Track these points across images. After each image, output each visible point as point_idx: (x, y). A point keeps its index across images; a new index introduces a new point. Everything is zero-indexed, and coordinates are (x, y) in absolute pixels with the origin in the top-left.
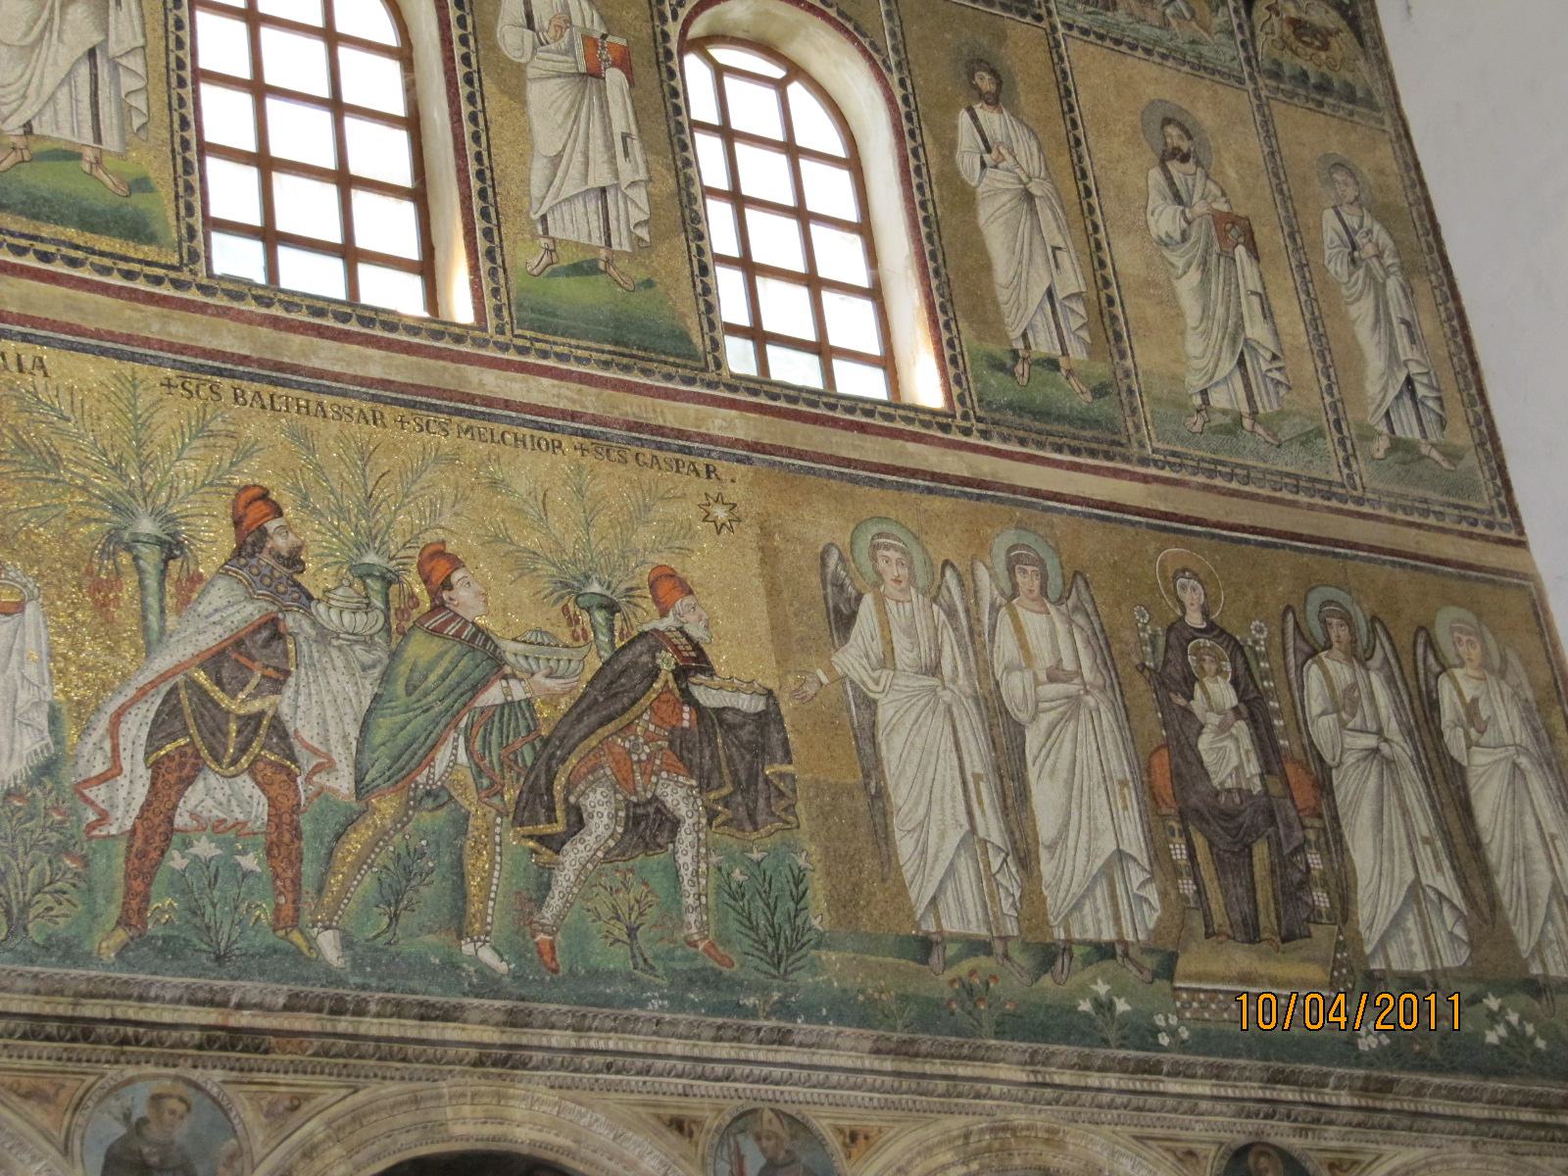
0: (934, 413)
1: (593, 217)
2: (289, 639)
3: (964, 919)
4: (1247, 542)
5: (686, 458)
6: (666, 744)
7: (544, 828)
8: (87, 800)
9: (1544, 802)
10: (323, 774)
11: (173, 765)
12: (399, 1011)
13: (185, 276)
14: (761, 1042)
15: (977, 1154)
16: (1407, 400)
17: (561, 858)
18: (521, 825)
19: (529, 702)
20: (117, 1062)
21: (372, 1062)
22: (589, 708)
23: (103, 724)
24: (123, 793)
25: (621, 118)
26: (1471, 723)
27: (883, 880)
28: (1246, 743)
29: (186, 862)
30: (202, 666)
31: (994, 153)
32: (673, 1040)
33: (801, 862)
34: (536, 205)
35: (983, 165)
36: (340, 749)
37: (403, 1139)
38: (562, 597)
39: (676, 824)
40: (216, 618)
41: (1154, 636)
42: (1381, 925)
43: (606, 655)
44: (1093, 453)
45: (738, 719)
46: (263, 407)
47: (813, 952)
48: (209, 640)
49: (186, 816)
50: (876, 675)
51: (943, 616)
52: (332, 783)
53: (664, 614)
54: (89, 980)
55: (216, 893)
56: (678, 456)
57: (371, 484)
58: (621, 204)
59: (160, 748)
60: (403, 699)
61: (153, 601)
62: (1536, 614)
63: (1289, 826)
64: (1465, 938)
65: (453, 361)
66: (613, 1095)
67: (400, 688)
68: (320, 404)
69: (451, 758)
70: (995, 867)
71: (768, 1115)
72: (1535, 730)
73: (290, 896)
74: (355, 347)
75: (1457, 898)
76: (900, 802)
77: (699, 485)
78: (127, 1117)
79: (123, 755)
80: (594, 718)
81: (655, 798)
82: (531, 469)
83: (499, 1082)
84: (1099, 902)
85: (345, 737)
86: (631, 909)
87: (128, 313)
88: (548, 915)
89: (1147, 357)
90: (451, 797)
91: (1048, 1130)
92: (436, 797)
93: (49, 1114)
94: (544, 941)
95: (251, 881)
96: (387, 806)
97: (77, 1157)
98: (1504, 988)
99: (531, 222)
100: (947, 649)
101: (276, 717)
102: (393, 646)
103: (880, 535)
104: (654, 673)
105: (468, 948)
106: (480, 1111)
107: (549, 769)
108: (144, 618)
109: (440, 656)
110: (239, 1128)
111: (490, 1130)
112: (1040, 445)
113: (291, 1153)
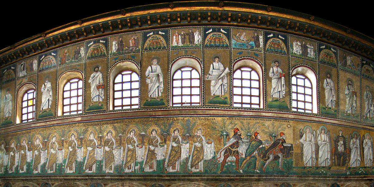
0: (316, 114)
3: (310, 165)
12: (247, 176)
23: (219, 153)
44: (333, 118)
48: (231, 144)
61: (225, 141)
67: (251, 147)
70: (314, 160)
77: (286, 123)
85: (244, 152)
89: (341, 107)
104: (279, 143)
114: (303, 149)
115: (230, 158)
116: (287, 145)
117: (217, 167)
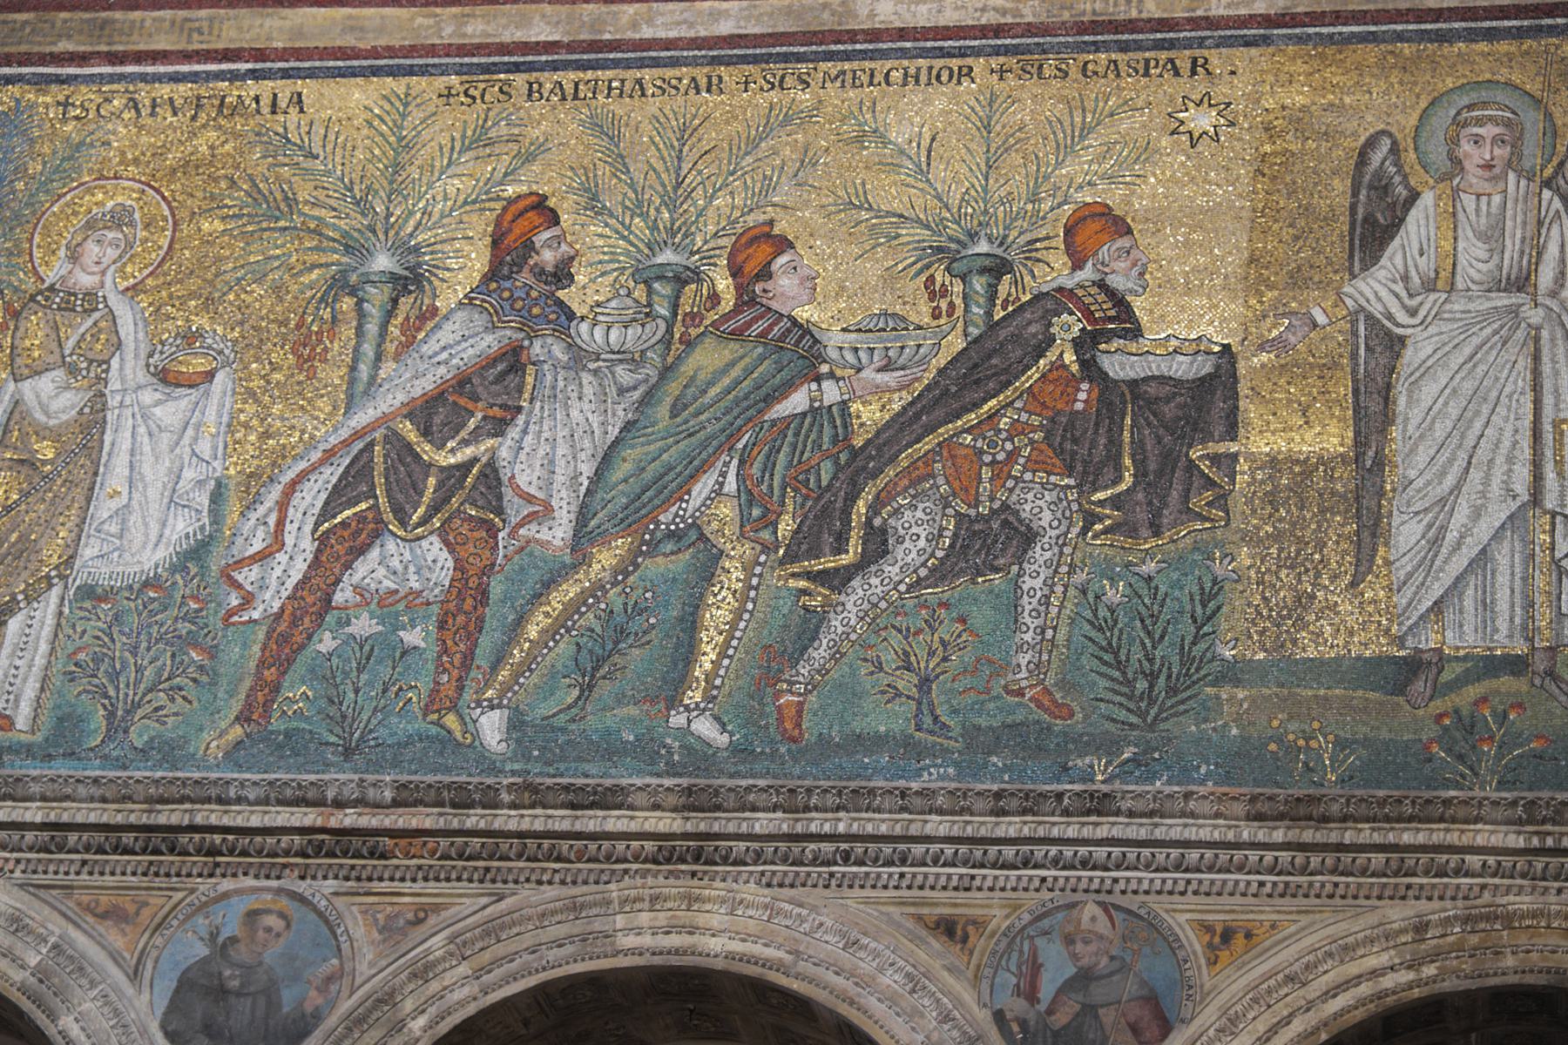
2: (530, 369)
5: (1163, 56)
6: (1038, 436)
7: (828, 562)
10: (534, 527)
11: (346, 534)
14: (1066, 813)
15: (1434, 956)
17: (842, 598)
20: (211, 875)
21: (521, 864)
22: (937, 401)
23: (275, 493)
27: (1353, 584)
29: (334, 644)
30: (410, 416)
32: (934, 817)
36: (564, 494)
37: (553, 954)
38: (928, 267)
39: (1029, 537)
40: (444, 355)
43: (974, 332)
48: (426, 385)
49: (349, 594)
50: (1413, 303)
51: (1557, 204)
52: (545, 535)
53: (1077, 266)
54: (157, 782)
55: (364, 677)
56: (1147, 55)
57: (686, 167)
59: (334, 517)
61: (368, 349)
66: (857, 892)
67: (663, 411)
68: (639, 82)
76: (1412, 474)
79: (288, 527)
80: (939, 413)
81: (1005, 507)
82: (920, 112)
83: (696, 882)
85: (576, 476)
87: (419, 20)
90: (702, 537)
92: (680, 538)
93: (124, 934)
94: (789, 703)
95: (409, 659)
96: (605, 559)
97: (146, 982)
102: (670, 360)
103: (1470, 107)
105: (678, 720)
106: (662, 918)
108: (353, 369)
109: (732, 364)
110: (345, 946)
111: (675, 941)
113: (395, 975)
114: (1387, 398)
116: (1157, 367)
117: (208, 676)
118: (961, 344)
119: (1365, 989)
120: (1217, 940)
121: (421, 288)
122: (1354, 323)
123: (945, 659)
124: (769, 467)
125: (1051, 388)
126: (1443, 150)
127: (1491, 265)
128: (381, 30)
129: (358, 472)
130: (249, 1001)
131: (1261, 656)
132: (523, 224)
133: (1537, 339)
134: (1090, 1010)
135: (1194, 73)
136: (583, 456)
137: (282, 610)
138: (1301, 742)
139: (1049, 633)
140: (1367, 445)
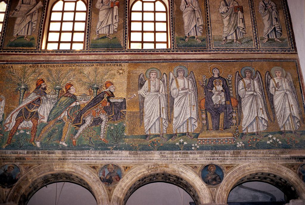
1: (107, 30)
2: (42, 100)
3: (155, 131)
4: (231, 61)
5: (116, 64)
8: (5, 126)
9: (291, 99)
10: (42, 119)
13: (37, 50)
16: (274, 32)
17: (80, 128)
18: (74, 124)
19: (80, 105)
23: (10, 115)
24: (11, 125)
25: (115, 13)
26: (277, 87)
27: (140, 126)
28: (223, 96)
30: (27, 106)
31: (188, 5)
33: (124, 125)
34: (97, 29)
35: (185, 7)
39: (102, 121)
40: (31, 98)
41: (207, 80)
42: (247, 125)
43: (95, 96)
45: (118, 103)
46: (45, 67)
47: (124, 139)
48: (29, 102)
50: (146, 93)
51: (162, 82)
52: (44, 120)
58: (113, 26)
60: (58, 107)
61: (21, 98)
62: (297, 66)
63: (229, 109)
64: (266, 125)
65: (78, 55)
68: (54, 65)
69: (65, 114)
70: (163, 122)
71: (111, 165)
72: (292, 87)
73: (33, 137)
74: (62, 56)
75: (266, 118)
78: (4, 170)
81: (99, 117)
82: (88, 70)
84: (184, 126)
86: (91, 135)
87: (27, 57)
88: (76, 137)
91: (165, 165)
98: (273, 134)
99: (96, 32)
100: (161, 87)
101: (37, 112)
105: (61, 143)
107: (81, 115)
108: (20, 100)
109: (66, 100)
111: (61, 169)
112: (188, 51)
115: (24, 123)
116: (116, 101)
118: (93, 98)
119: (142, 173)
120: (125, 168)
121: (28, 90)
122: (139, 96)
123: (93, 135)
124: (71, 112)
125: (104, 103)
126: (149, 76)
127: (155, 89)
128: (22, 58)
129: (21, 112)
130: (9, 178)
131: (129, 135)
132: (40, 83)
133: (160, 98)
134: (111, 177)
135: (120, 66)
136: (48, 111)
137: (12, 129)
138: (134, 145)
139: (105, 132)
140: (141, 110)
